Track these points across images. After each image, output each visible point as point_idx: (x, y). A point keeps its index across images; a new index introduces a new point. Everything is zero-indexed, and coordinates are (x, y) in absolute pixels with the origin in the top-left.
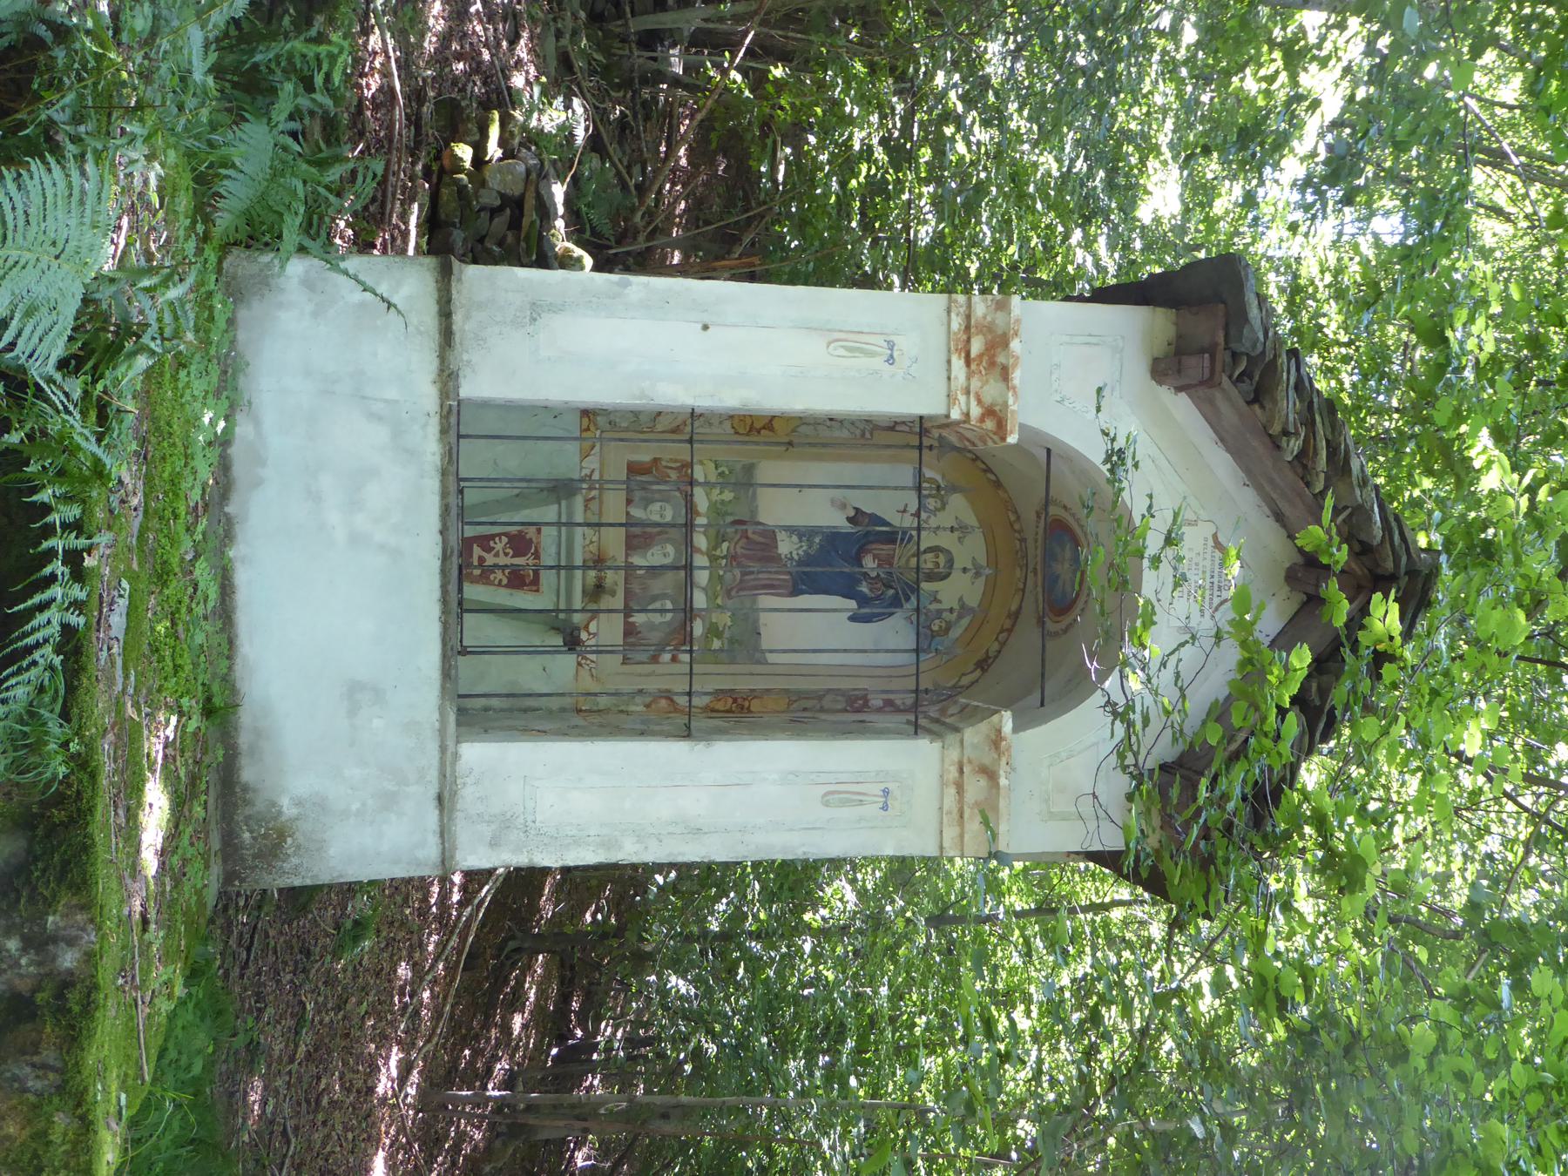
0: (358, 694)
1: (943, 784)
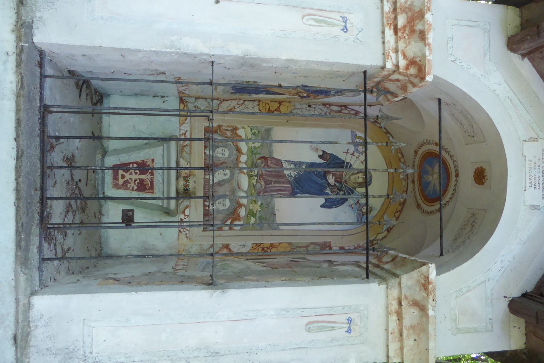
1: (388, 314)
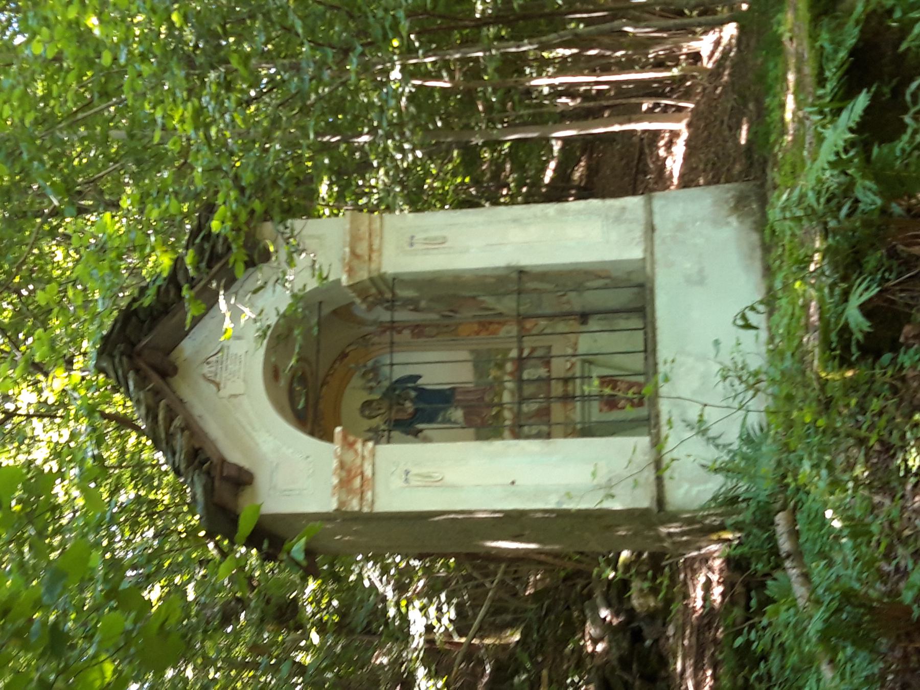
0: (699, 280)
1: (380, 250)
